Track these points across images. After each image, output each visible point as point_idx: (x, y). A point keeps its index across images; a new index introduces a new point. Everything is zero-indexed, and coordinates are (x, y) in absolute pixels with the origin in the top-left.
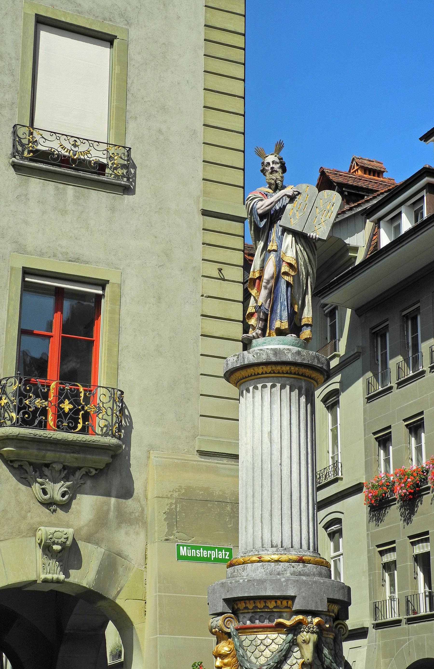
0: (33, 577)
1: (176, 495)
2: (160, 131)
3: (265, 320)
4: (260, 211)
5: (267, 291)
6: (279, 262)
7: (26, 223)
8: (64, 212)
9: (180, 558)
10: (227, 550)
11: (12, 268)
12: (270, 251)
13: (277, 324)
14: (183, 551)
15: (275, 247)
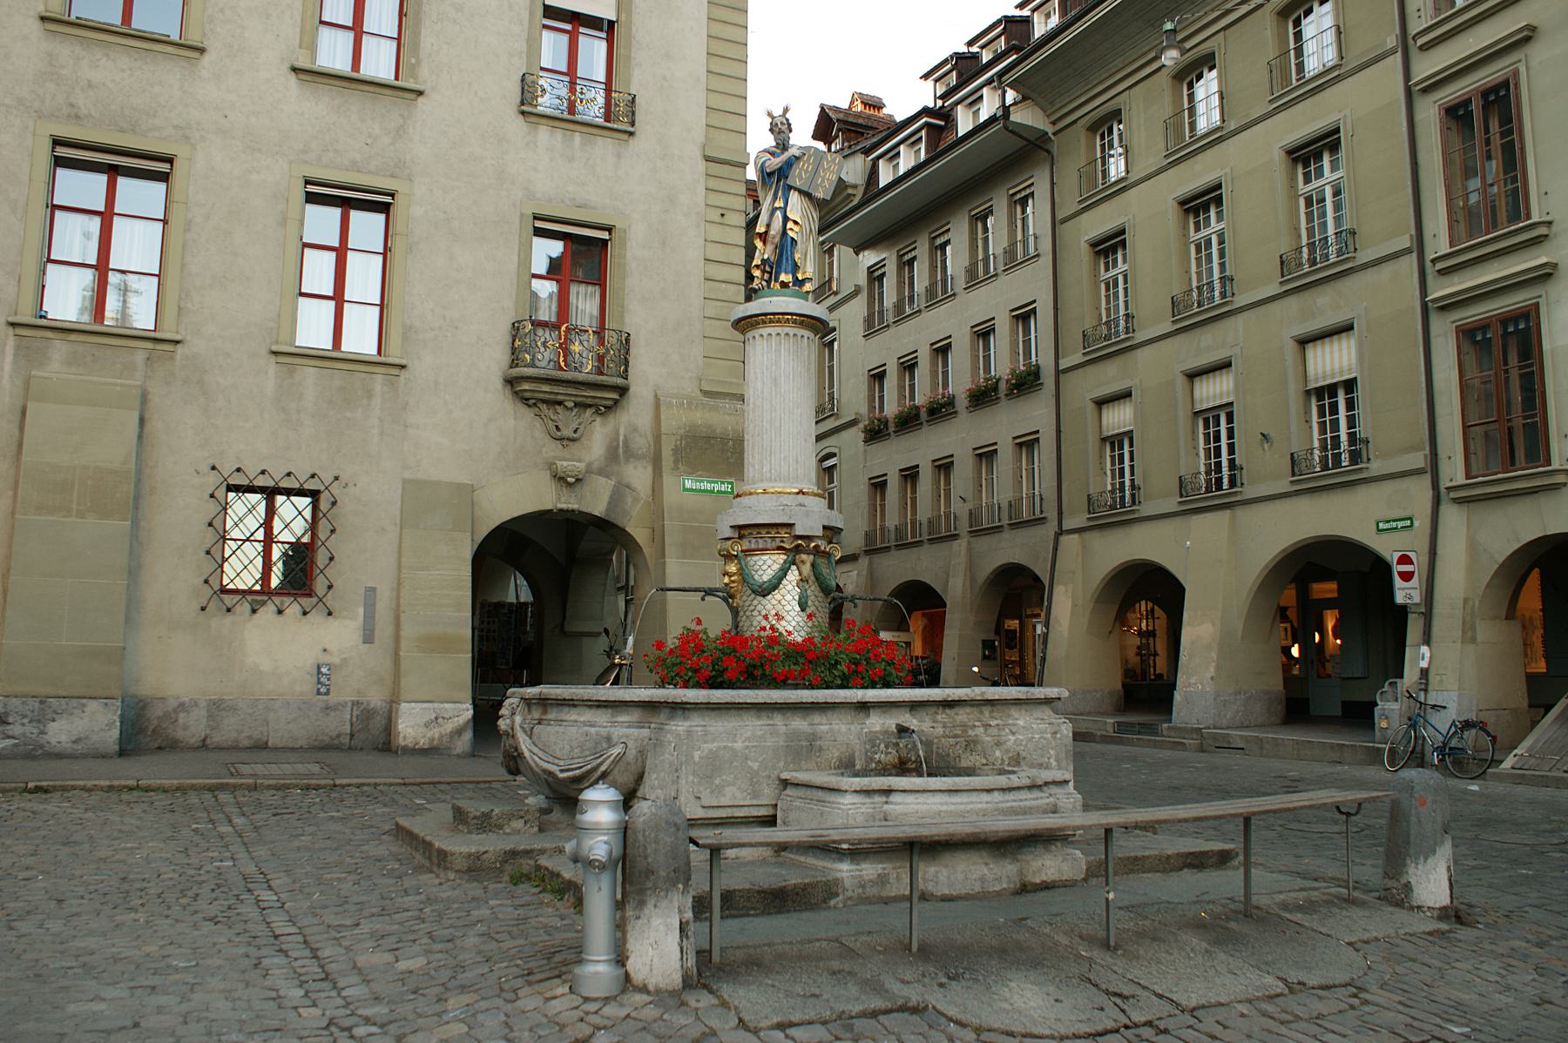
0: (549, 507)
1: (682, 431)
2: (664, 78)
3: (771, 273)
4: (768, 170)
5: (773, 247)
6: (786, 219)
7: (535, 169)
8: (571, 159)
9: (685, 489)
10: (728, 483)
11: (522, 215)
12: (777, 208)
13: (783, 277)
14: (688, 484)
15: (782, 205)
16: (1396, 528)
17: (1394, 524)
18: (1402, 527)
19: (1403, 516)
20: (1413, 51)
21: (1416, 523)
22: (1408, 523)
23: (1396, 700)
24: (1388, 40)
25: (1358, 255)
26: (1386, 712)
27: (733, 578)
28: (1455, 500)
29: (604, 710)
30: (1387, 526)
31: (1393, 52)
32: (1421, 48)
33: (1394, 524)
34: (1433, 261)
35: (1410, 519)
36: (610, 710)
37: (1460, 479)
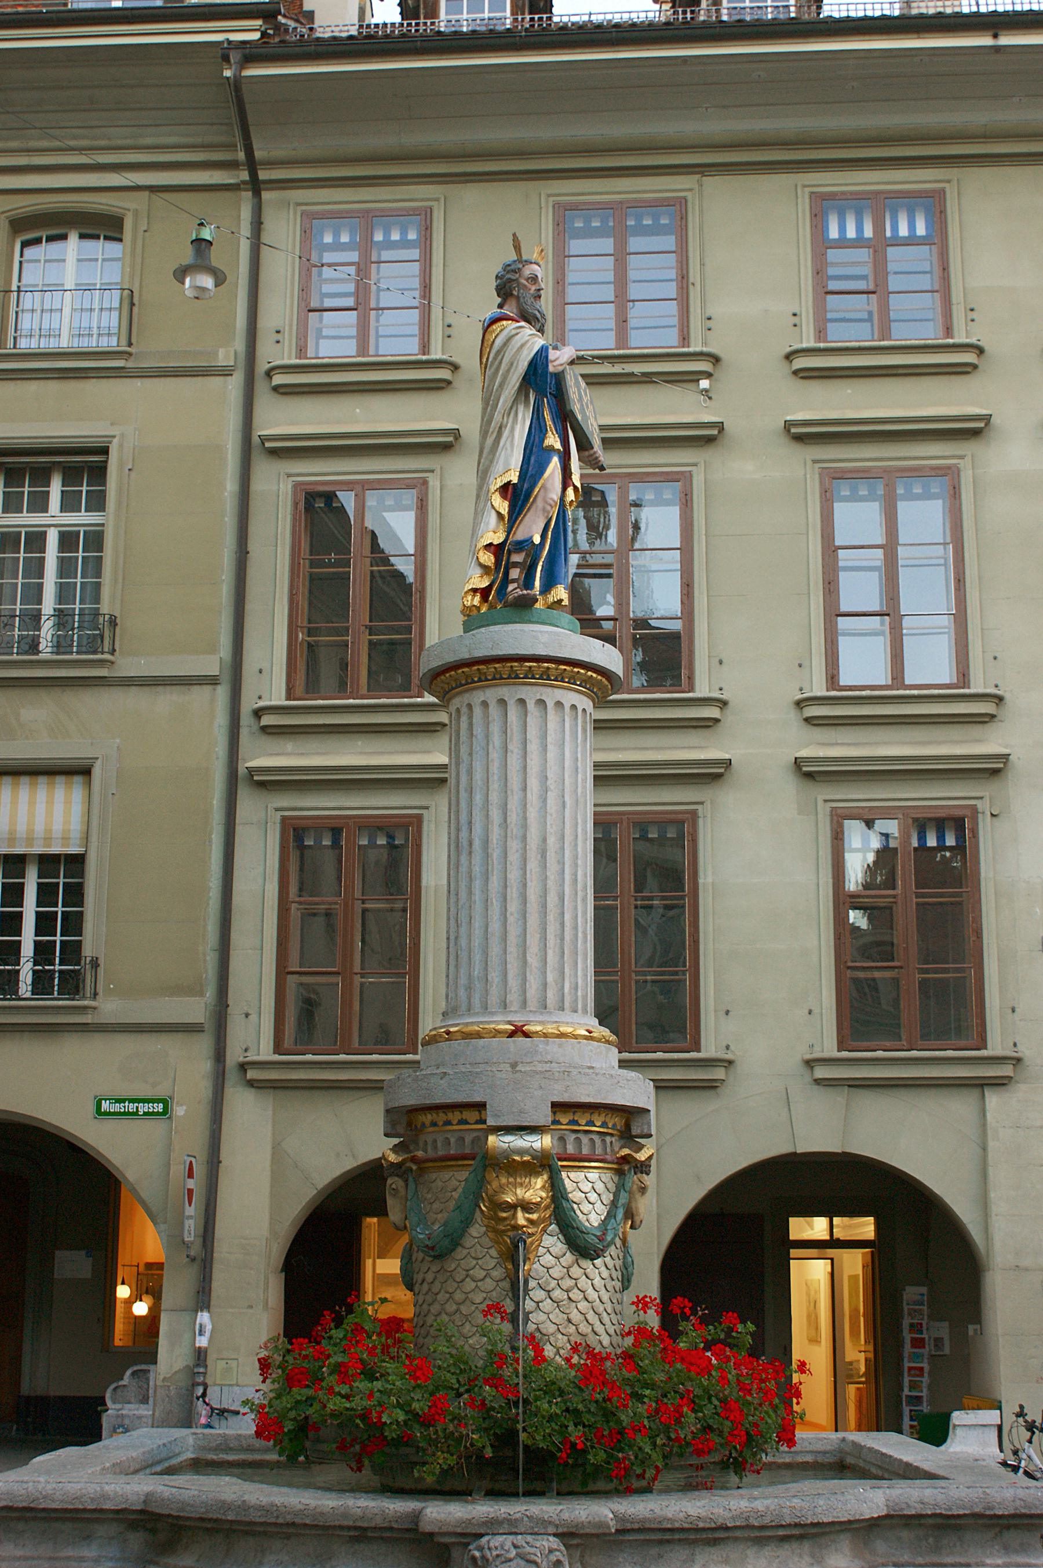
16: (136, 1113)
17: (132, 1107)
18: (145, 1114)
19: (149, 1093)
20: (261, 388)
21: (179, 1111)
22: (160, 1107)
23: (145, 1400)
24: (221, 352)
25: (117, 658)
26: (127, 1421)
27: (534, 1216)
28: (251, 1084)
29: (795, 1545)
30: (117, 1107)
31: (225, 372)
32: (276, 389)
33: (132, 1107)
34: (258, 713)
35: (165, 1102)
36: (806, 1545)
37: (265, 1052)
